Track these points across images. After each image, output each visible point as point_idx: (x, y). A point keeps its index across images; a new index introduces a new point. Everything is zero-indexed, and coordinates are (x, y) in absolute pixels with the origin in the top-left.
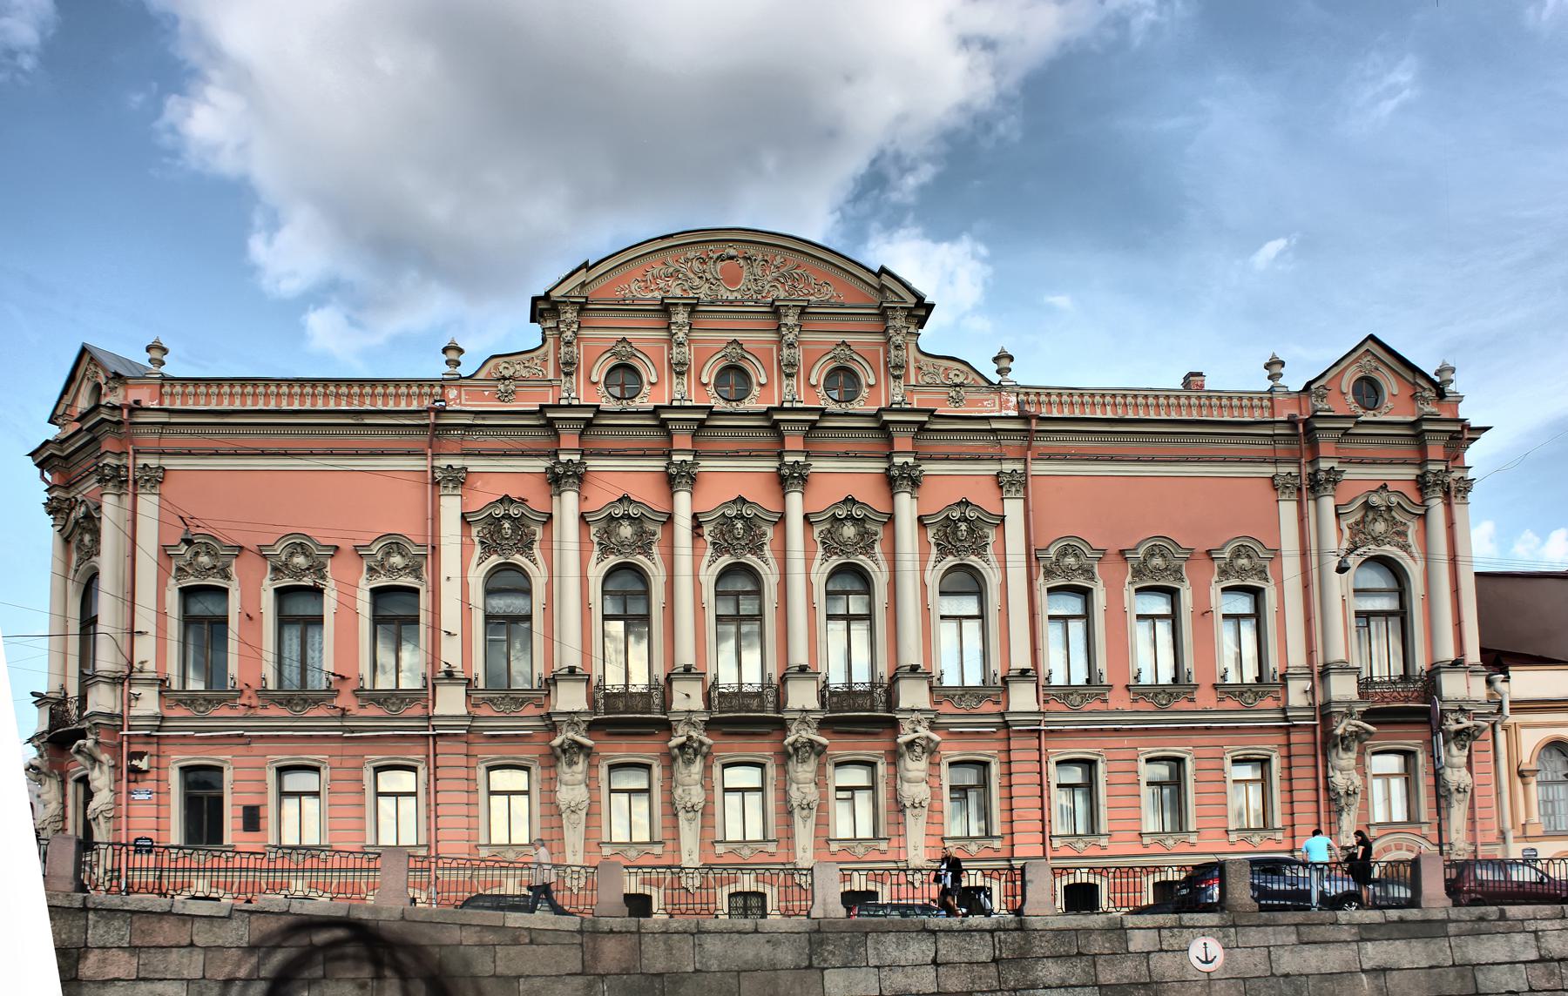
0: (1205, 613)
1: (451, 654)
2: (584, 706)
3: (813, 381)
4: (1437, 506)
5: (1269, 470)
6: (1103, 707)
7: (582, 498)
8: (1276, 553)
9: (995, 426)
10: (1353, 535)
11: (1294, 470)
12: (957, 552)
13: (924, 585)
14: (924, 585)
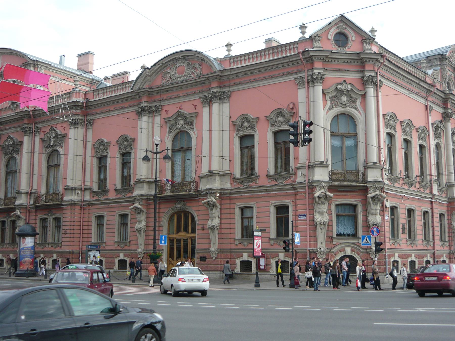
4: (371, 91)
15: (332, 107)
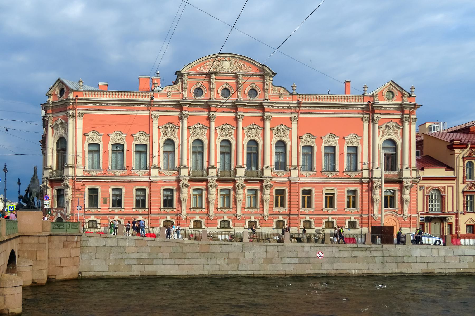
0: (342, 154)
1: (155, 161)
2: (187, 175)
3: (246, 93)
4: (407, 126)
5: (361, 116)
7: (188, 123)
8: (362, 137)
9: (291, 105)
10: (383, 133)
11: (368, 116)
13: (271, 145)
14: (271, 145)
15: (383, 136)
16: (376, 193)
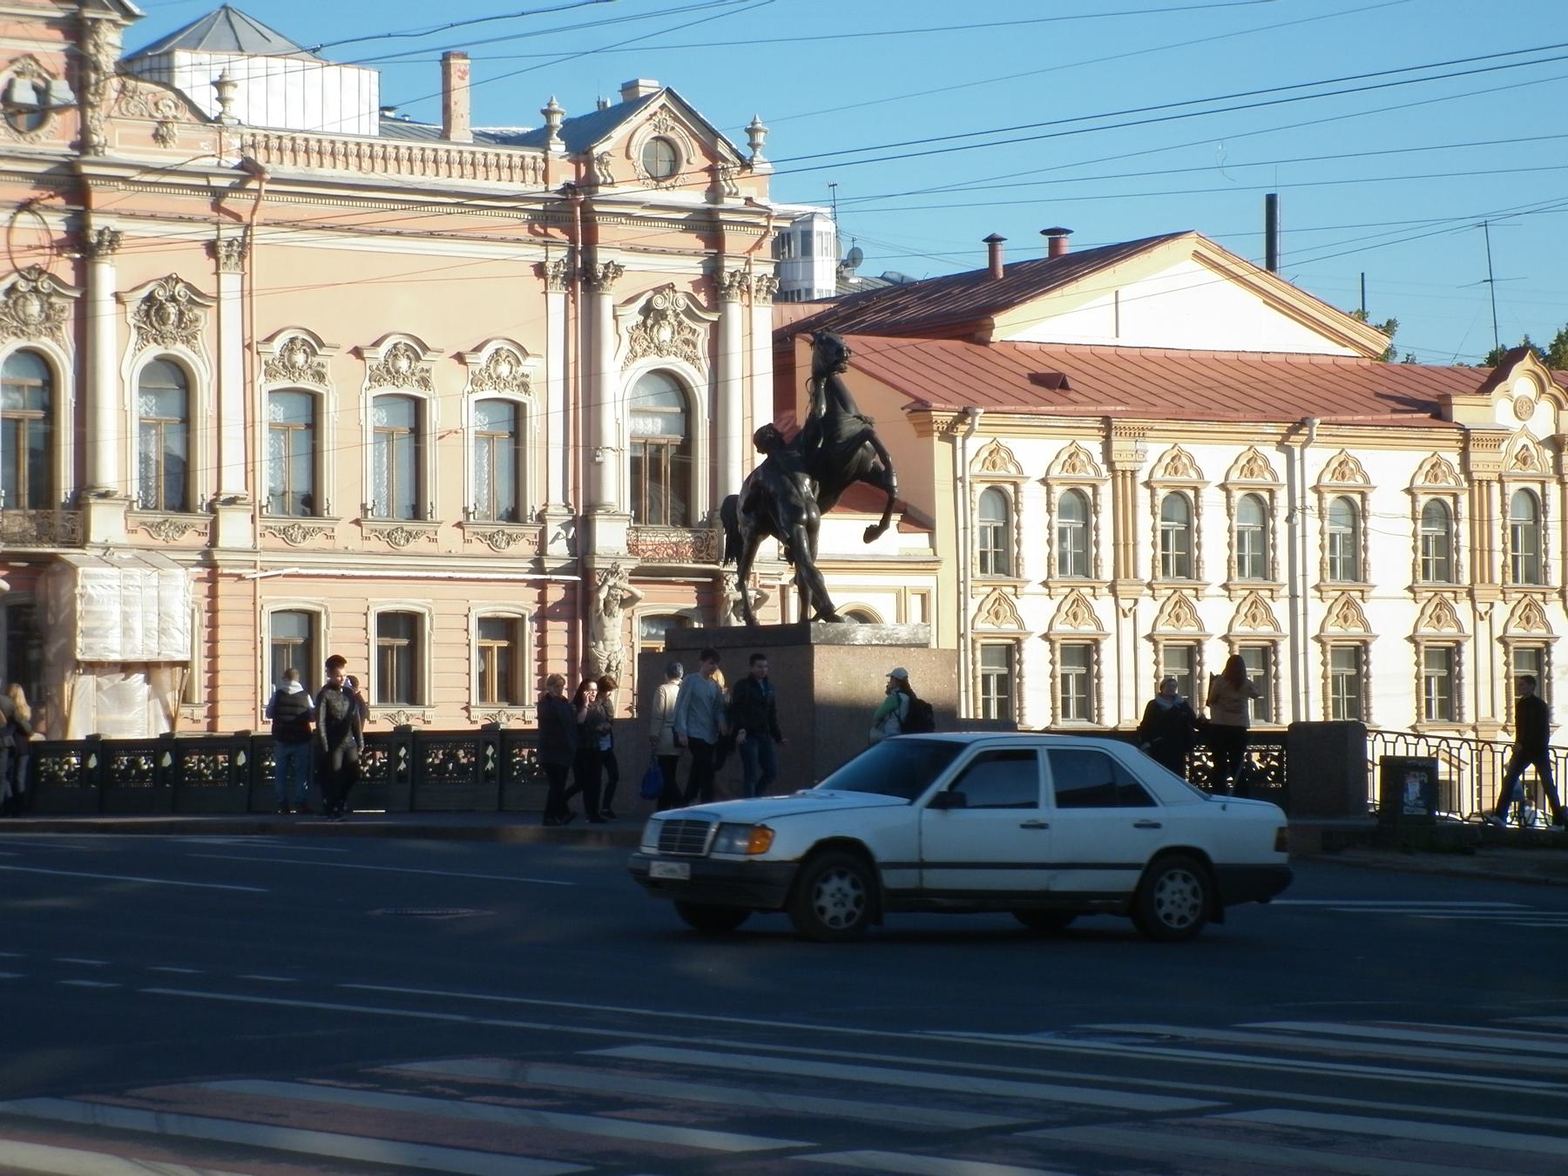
6: (328, 544)
12: (160, 338)
16: (609, 633)
